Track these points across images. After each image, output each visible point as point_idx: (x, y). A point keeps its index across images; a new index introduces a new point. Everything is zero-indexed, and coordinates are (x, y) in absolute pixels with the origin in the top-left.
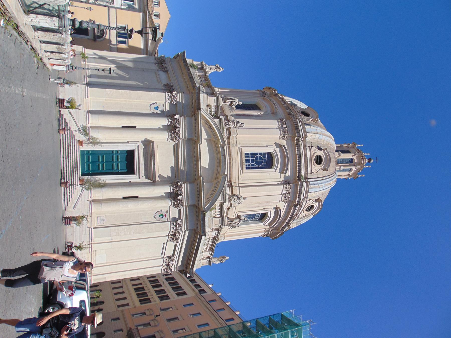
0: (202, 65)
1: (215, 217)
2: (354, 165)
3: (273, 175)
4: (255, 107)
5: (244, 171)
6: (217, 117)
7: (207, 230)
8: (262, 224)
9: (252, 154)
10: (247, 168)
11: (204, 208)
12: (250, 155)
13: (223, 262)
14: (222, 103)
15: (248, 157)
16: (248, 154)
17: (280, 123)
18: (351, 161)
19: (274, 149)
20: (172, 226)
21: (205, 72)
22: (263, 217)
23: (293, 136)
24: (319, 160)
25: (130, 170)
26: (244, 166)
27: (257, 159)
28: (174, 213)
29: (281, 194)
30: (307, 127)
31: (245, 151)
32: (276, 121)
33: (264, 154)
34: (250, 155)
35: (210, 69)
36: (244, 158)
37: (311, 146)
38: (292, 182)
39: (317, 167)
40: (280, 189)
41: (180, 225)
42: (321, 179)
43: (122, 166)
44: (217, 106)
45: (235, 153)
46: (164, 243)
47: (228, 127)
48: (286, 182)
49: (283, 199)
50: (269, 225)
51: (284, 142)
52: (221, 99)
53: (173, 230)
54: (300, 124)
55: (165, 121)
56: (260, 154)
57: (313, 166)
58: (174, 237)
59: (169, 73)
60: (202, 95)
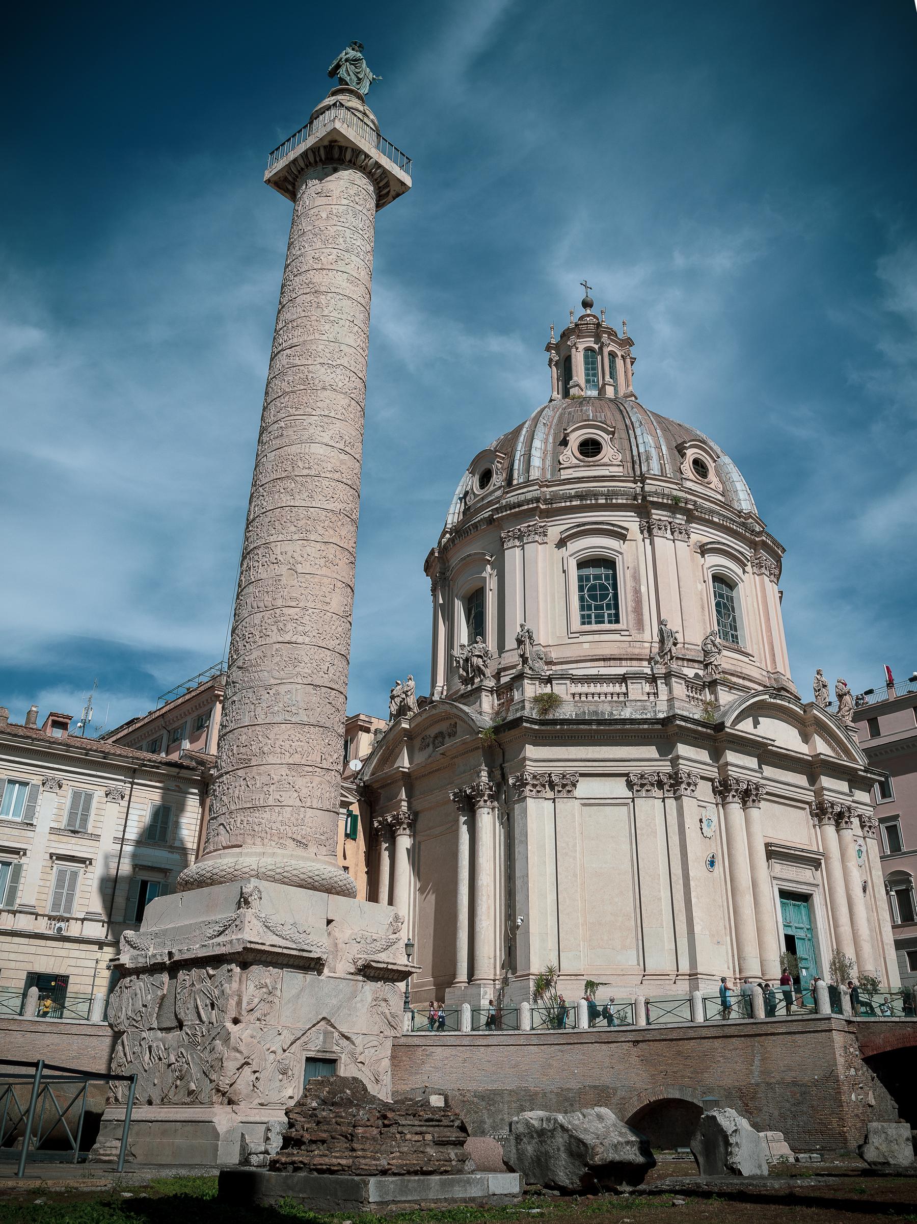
5: (625, 628)
9: (582, 608)
10: (617, 621)
12: (586, 612)
15: (589, 616)
16: (583, 617)
24: (590, 448)
26: (614, 626)
27: (593, 597)
31: (576, 625)
33: (580, 578)
34: (586, 612)
36: (595, 627)
39: (608, 452)
40: (663, 544)
42: (633, 440)
45: (587, 646)
48: (648, 530)
50: (743, 565)
51: (555, 531)
56: (581, 589)
57: (606, 460)
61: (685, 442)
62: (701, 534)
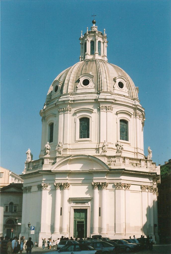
0: (27, 163)
1: (115, 162)
2: (96, 40)
3: (93, 118)
4: (51, 126)
6: (56, 158)
7: (122, 167)
8: (129, 122)
11: (107, 170)
13: (151, 151)
14: (48, 156)
17: (60, 113)
18: (93, 43)
19: (77, 118)
20: (118, 188)
21: (31, 162)
22: (124, 122)
23: (69, 104)
24: (86, 82)
25: (85, 211)
28: (110, 186)
29: (107, 112)
30: (64, 91)
32: (60, 115)
35: (29, 158)
37: (76, 89)
38: (99, 104)
39: (91, 84)
41: (117, 184)
43: (83, 215)
44: (50, 158)
46: (131, 192)
47: (62, 152)
48: (99, 110)
49: (110, 111)
51: (73, 110)
52: (45, 156)
53: (121, 188)
54: (62, 99)
55: (58, 191)
57: (90, 87)
58: (127, 186)
59: (32, 185)
60: (44, 169)
61: (116, 77)
62: (116, 109)
